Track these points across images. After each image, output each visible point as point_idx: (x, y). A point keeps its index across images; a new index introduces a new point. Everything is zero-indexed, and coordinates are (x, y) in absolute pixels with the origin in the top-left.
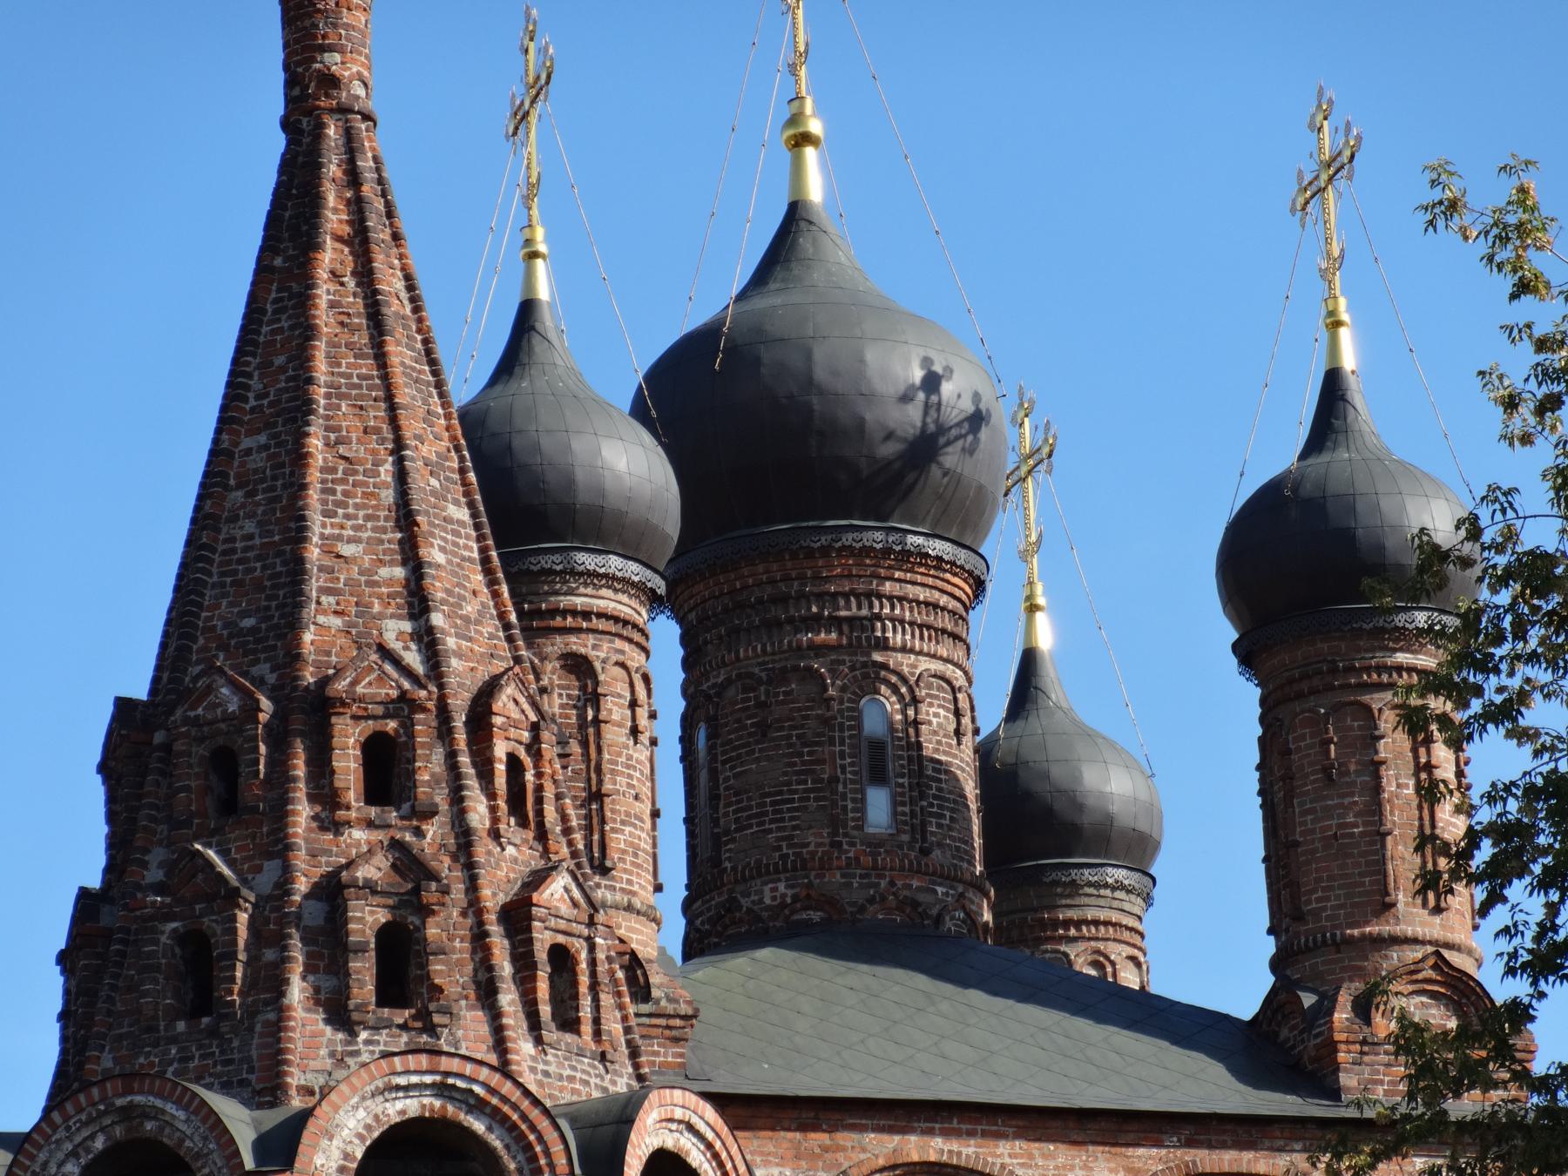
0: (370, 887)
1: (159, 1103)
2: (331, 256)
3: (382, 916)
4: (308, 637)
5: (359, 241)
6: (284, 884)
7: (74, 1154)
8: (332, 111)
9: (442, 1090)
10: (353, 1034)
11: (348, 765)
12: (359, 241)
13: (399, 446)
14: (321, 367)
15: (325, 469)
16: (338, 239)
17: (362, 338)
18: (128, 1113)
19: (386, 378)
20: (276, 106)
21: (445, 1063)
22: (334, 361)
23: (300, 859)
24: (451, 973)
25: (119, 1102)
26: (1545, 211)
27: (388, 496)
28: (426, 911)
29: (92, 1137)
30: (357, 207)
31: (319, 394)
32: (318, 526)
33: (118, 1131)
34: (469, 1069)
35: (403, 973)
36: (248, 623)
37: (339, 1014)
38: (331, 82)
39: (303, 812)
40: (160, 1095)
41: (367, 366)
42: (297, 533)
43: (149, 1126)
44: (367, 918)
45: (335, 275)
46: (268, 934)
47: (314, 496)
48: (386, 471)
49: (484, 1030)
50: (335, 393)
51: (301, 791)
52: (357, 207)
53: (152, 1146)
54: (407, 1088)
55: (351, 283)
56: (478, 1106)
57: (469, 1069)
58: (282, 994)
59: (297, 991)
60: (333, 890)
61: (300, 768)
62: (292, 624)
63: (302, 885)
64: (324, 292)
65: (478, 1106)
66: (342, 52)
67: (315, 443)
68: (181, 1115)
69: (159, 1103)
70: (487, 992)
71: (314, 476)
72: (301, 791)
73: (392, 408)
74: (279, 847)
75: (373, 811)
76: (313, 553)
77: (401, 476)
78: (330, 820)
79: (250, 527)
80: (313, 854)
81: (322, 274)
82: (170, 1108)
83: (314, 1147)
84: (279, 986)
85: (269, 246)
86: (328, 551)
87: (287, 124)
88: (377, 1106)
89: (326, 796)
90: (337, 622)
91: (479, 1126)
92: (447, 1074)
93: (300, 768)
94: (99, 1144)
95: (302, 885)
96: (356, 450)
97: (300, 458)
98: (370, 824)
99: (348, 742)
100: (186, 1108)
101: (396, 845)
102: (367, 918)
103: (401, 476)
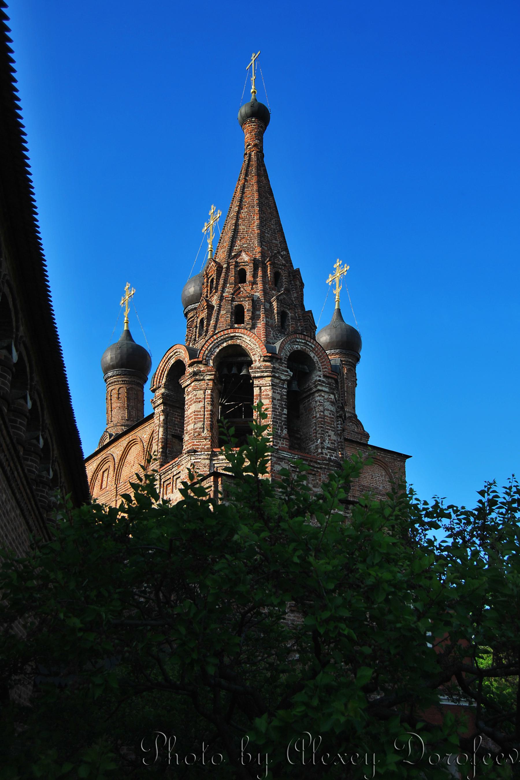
43: (238, 341)
53: (239, 346)
68: (249, 339)
82: (245, 337)
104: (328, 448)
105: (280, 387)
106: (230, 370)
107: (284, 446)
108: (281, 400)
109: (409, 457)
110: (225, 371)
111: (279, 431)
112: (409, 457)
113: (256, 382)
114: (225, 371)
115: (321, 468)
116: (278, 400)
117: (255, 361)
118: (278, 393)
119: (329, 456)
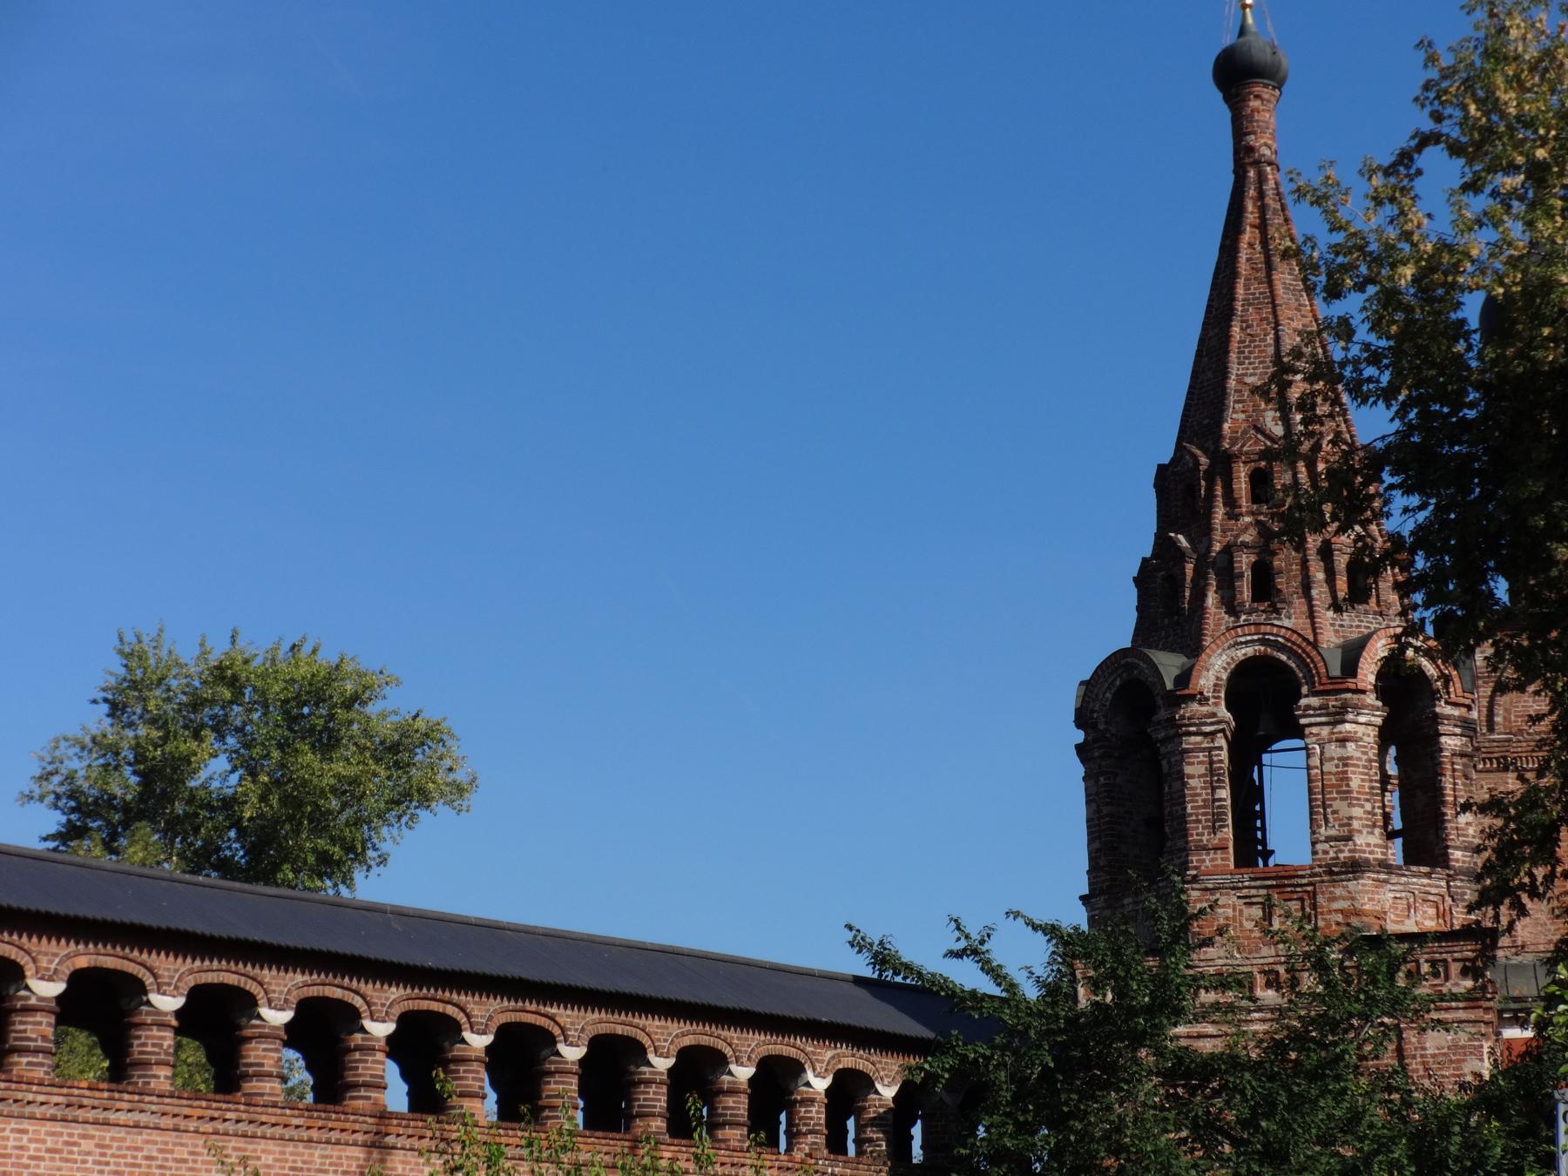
0: (1245, 545)
2: (1248, 235)
3: (1253, 558)
4: (1226, 426)
5: (1263, 226)
6: (1210, 545)
7: (1109, 688)
8: (1251, 164)
9: (1263, 642)
10: (1238, 618)
11: (1242, 484)
12: (1263, 226)
13: (1277, 324)
14: (1240, 291)
15: (1241, 342)
16: (1253, 226)
17: (1261, 275)
19: (1272, 291)
20: (1230, 165)
21: (1263, 629)
22: (1247, 287)
23: (1217, 535)
24: (1286, 583)
26: (1344, 186)
27: (1271, 350)
28: (1274, 554)
30: (1263, 210)
31: (1239, 306)
32: (1235, 369)
34: (1275, 630)
35: (1265, 587)
37: (1232, 608)
38: (1251, 149)
39: (1220, 512)
41: (1264, 288)
42: (1224, 374)
44: (1244, 561)
45: (1251, 245)
46: (1200, 575)
47: (1233, 356)
48: (1270, 339)
49: (1305, 608)
50: (1247, 303)
51: (1219, 502)
52: (1263, 210)
54: (1246, 643)
55: (1258, 247)
56: (1281, 648)
57: (1275, 630)
58: (1204, 601)
59: (1211, 599)
60: (1228, 550)
61: (1219, 491)
62: (1219, 421)
63: (1217, 547)
64: (1243, 256)
65: (1281, 648)
66: (1255, 133)
67: (1236, 330)
70: (1306, 586)
71: (1234, 345)
72: (1219, 502)
73: (1274, 306)
74: (1208, 530)
76: (1232, 383)
77: (1277, 339)
78: (1233, 515)
79: (1210, 374)
80: (1224, 531)
81: (1244, 245)
83: (1199, 677)
84: (1203, 596)
85: (1225, 237)
86: (1240, 381)
87: (1235, 172)
88: (1232, 653)
89: (1231, 502)
90: (1243, 416)
91: (1284, 658)
93: (1219, 491)
95: (1217, 547)
96: (1256, 330)
97: (1227, 338)
98: (1252, 513)
101: (1258, 523)
102: (1244, 561)
103: (1277, 339)
104: (1328, 839)
105: (1203, 750)
113: (1163, 750)
119: (1332, 854)
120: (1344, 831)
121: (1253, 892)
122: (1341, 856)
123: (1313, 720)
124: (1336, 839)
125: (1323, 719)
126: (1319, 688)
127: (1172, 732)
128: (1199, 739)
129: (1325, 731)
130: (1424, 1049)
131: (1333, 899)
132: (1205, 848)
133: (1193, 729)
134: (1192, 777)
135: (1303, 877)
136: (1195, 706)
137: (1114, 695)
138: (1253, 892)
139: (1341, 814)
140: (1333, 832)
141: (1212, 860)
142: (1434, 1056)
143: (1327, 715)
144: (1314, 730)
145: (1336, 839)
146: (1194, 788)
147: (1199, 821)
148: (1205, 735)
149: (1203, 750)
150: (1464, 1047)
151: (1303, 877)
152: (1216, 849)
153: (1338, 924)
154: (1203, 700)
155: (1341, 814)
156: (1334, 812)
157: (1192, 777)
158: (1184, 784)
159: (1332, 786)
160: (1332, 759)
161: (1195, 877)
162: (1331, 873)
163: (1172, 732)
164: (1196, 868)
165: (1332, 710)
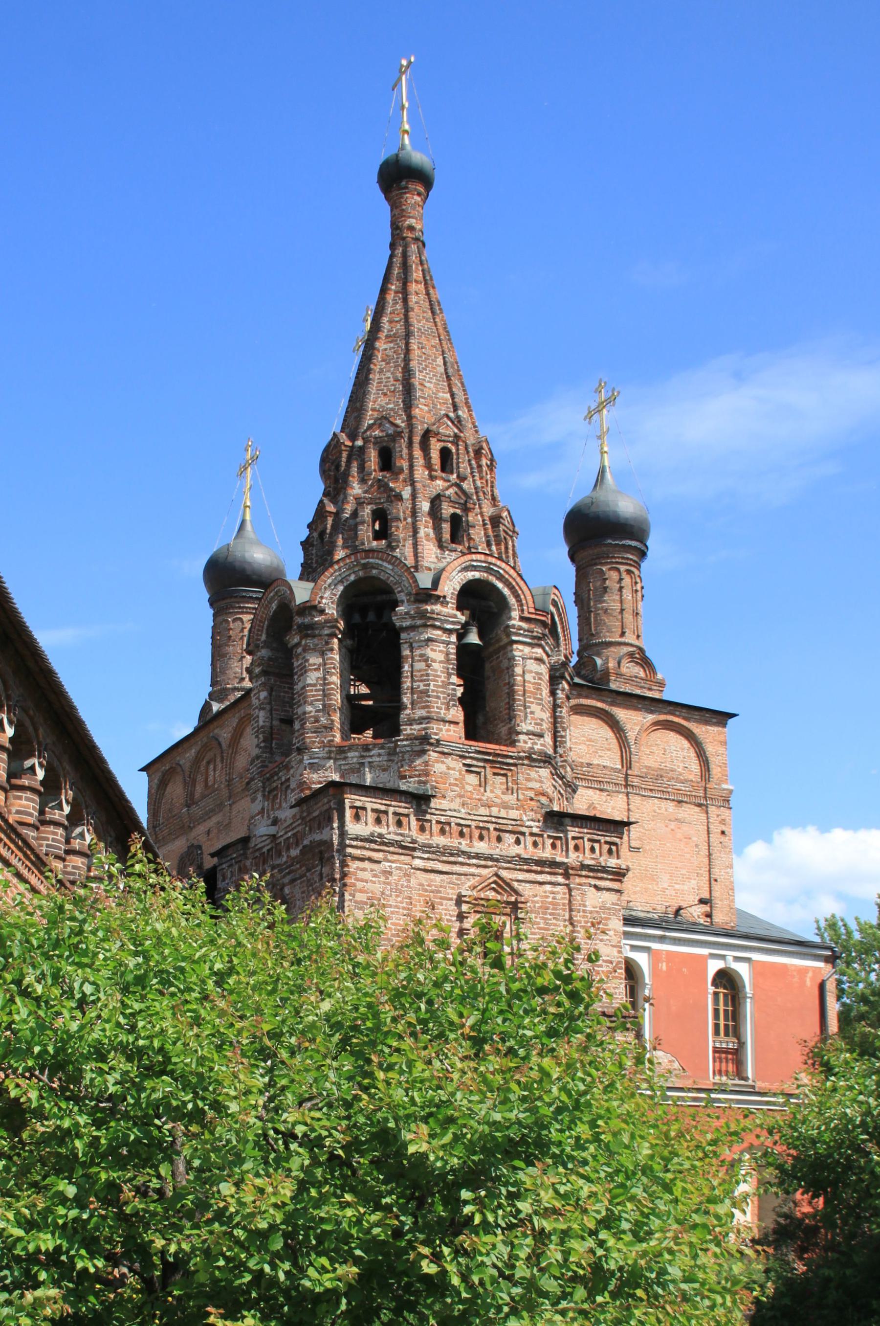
1: (380, 562)
18: (365, 567)
25: (363, 561)
29: (349, 575)
33: (361, 574)
36: (391, 406)
40: (382, 559)
43: (374, 572)
65: (500, 578)
68: (390, 567)
69: (380, 562)
75: (444, 475)
82: (385, 564)
90: (426, 408)
91: (500, 585)
92: (490, 563)
94: (352, 578)
99: (435, 447)
100: (393, 564)
102: (447, 510)
105: (443, 642)
106: (364, 616)
107: (452, 733)
108: (448, 660)
109: (733, 715)
110: (357, 618)
111: (443, 712)
112: (733, 715)
113: (403, 636)
114: (357, 618)
115: (515, 765)
116: (440, 662)
117: (402, 602)
118: (440, 651)
119: (529, 745)
120: (537, 729)
121: (475, 763)
122: (536, 747)
123: (521, 639)
124: (534, 734)
125: (528, 640)
126: (526, 614)
127: (419, 622)
128: (439, 632)
129: (527, 650)
130: (585, 906)
131: (529, 780)
132: (444, 721)
133: (438, 623)
134: (435, 661)
135: (511, 757)
136: (438, 608)
137: (346, 588)
138: (475, 763)
139: (536, 715)
140: (530, 728)
141: (448, 730)
142: (591, 912)
143: (533, 638)
144: (520, 647)
145: (534, 734)
146: (436, 671)
147: (438, 697)
148: (445, 630)
149: (443, 642)
150: (609, 909)
151: (511, 757)
152: (451, 722)
153: (532, 799)
154: (445, 603)
155: (536, 715)
156: (532, 713)
157: (435, 661)
158: (428, 666)
159: (531, 692)
160: (531, 672)
161: (438, 741)
162: (528, 758)
163: (419, 622)
164: (436, 734)
165: (535, 634)
